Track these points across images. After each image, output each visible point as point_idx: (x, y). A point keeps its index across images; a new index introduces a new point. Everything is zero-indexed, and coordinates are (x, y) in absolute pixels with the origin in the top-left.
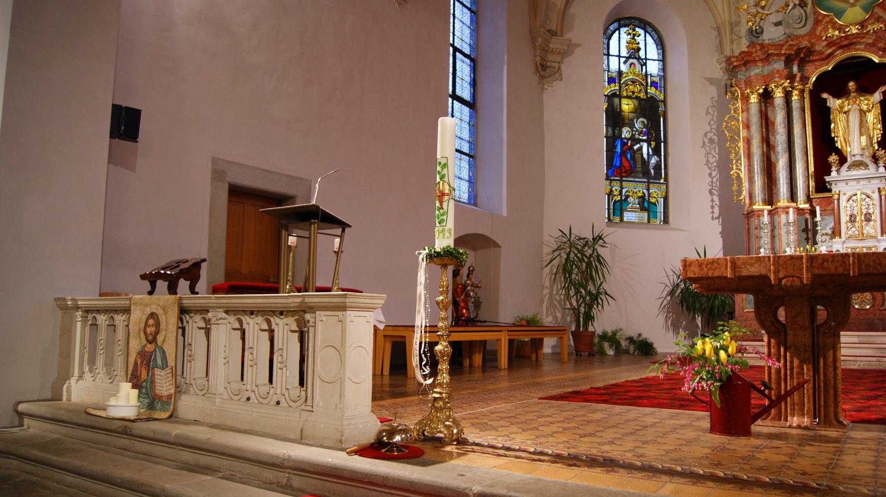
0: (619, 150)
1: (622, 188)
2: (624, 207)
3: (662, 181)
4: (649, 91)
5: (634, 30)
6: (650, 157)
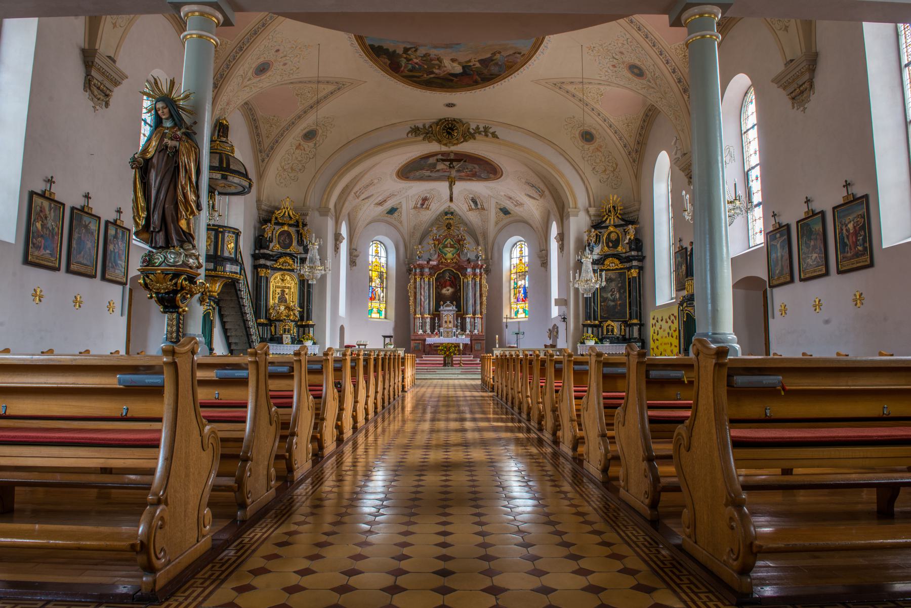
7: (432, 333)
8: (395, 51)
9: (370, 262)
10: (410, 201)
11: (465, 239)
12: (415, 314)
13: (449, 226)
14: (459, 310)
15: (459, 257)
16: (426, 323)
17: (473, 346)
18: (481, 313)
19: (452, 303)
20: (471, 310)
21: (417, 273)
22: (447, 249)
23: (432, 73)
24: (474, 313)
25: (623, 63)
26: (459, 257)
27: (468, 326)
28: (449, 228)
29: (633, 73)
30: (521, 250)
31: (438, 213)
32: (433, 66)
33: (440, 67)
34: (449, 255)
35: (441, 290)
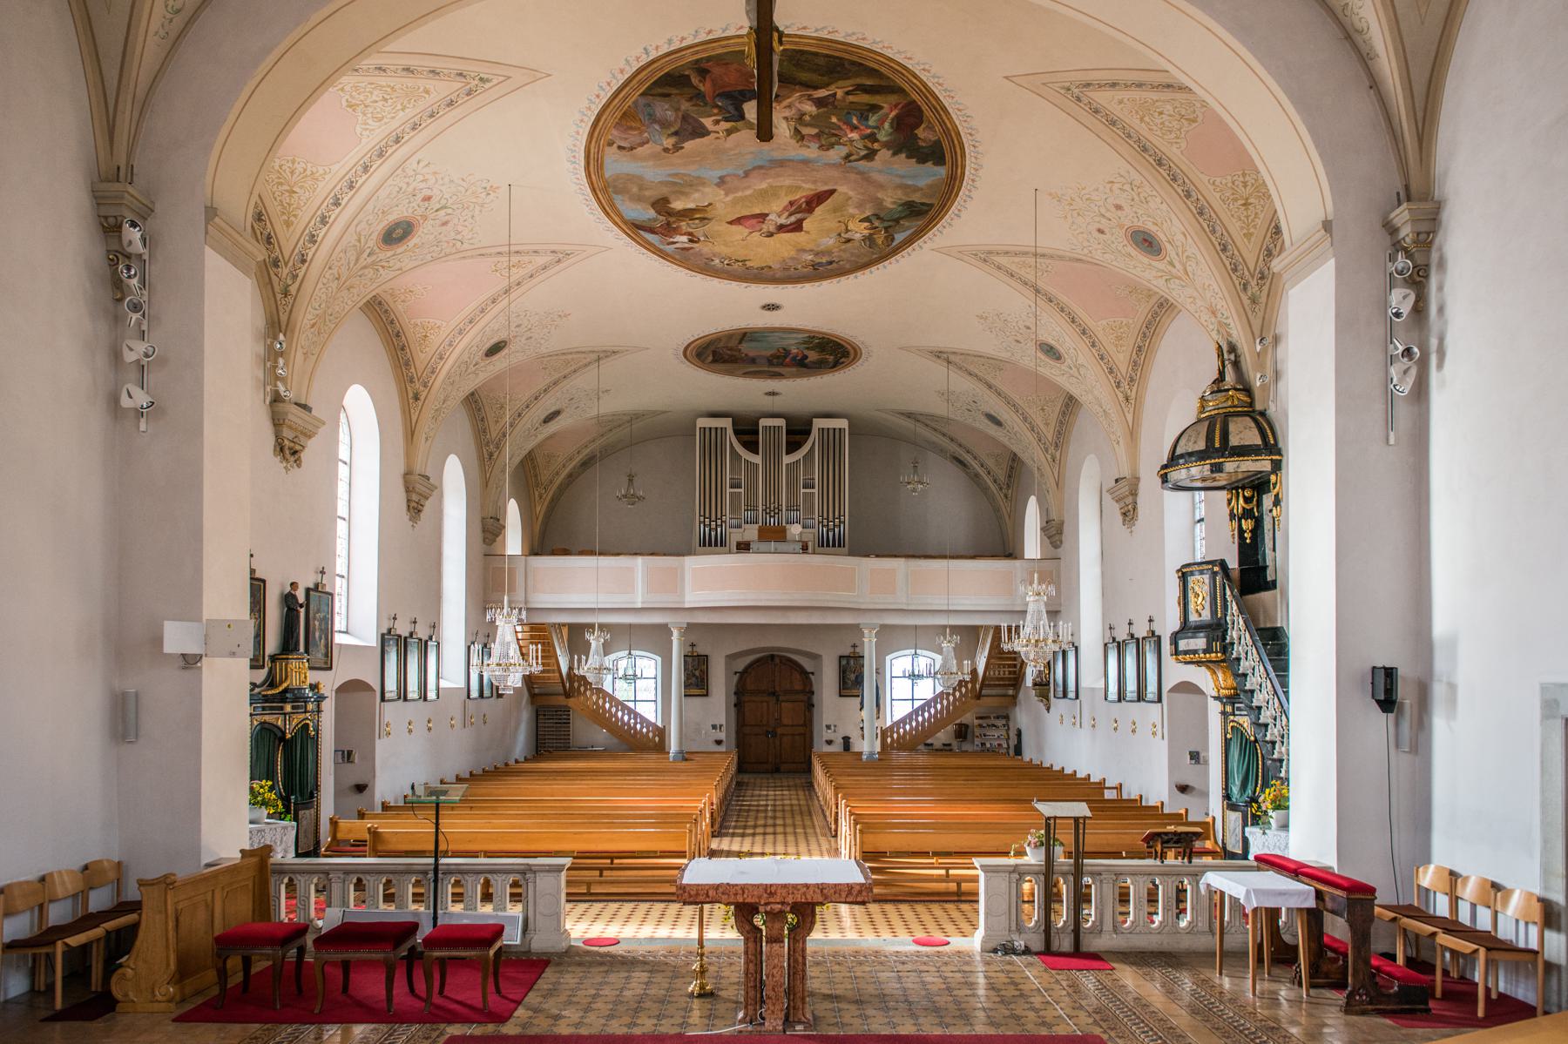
8: (894, 154)
23: (820, 103)
25: (425, 218)
29: (397, 225)
32: (815, 121)
33: (800, 118)
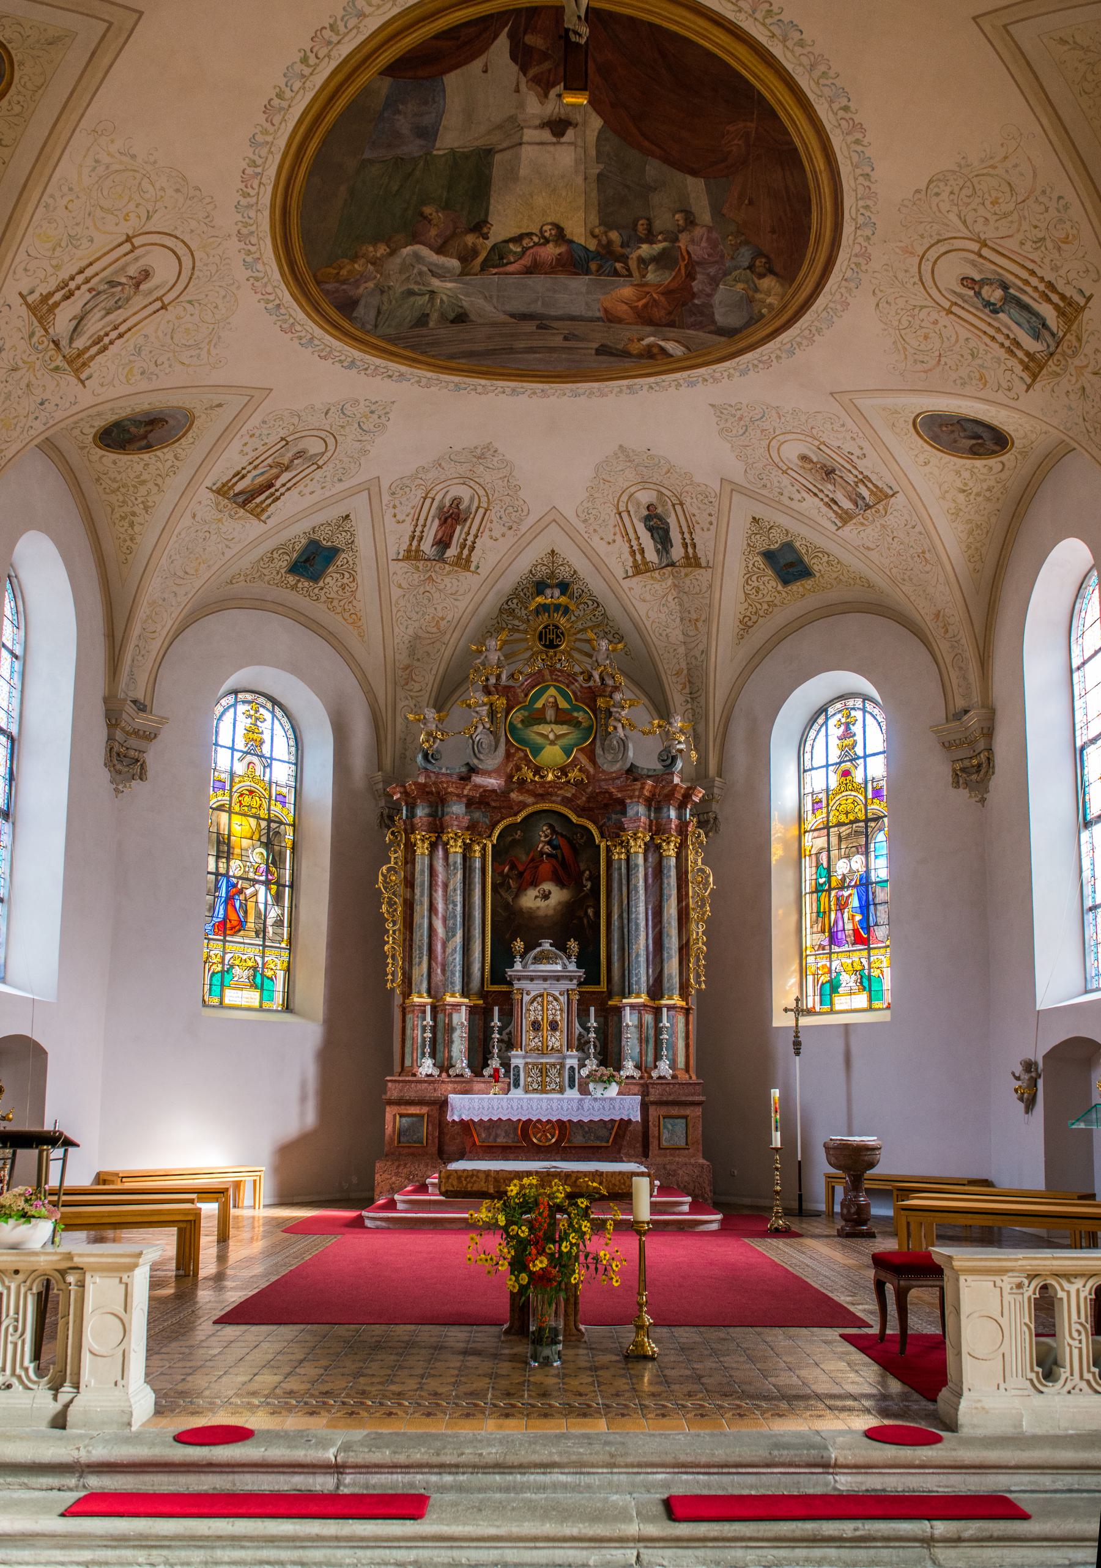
0: (224, 895)
1: (225, 953)
2: (226, 983)
3: (283, 945)
4: (272, 807)
5: (257, 711)
6: (269, 908)
7: (477, 1073)
9: (225, 776)
10: (388, 518)
11: (616, 688)
12: (407, 994)
13: (550, 639)
14: (592, 978)
15: (592, 759)
16: (450, 1029)
17: (654, 1131)
18: (684, 993)
19: (561, 946)
20: (642, 975)
21: (417, 820)
22: (544, 729)
24: (656, 990)
26: (592, 759)
27: (631, 1043)
28: (552, 645)
30: (848, 734)
31: (507, 584)
34: (552, 754)
35: (517, 896)
